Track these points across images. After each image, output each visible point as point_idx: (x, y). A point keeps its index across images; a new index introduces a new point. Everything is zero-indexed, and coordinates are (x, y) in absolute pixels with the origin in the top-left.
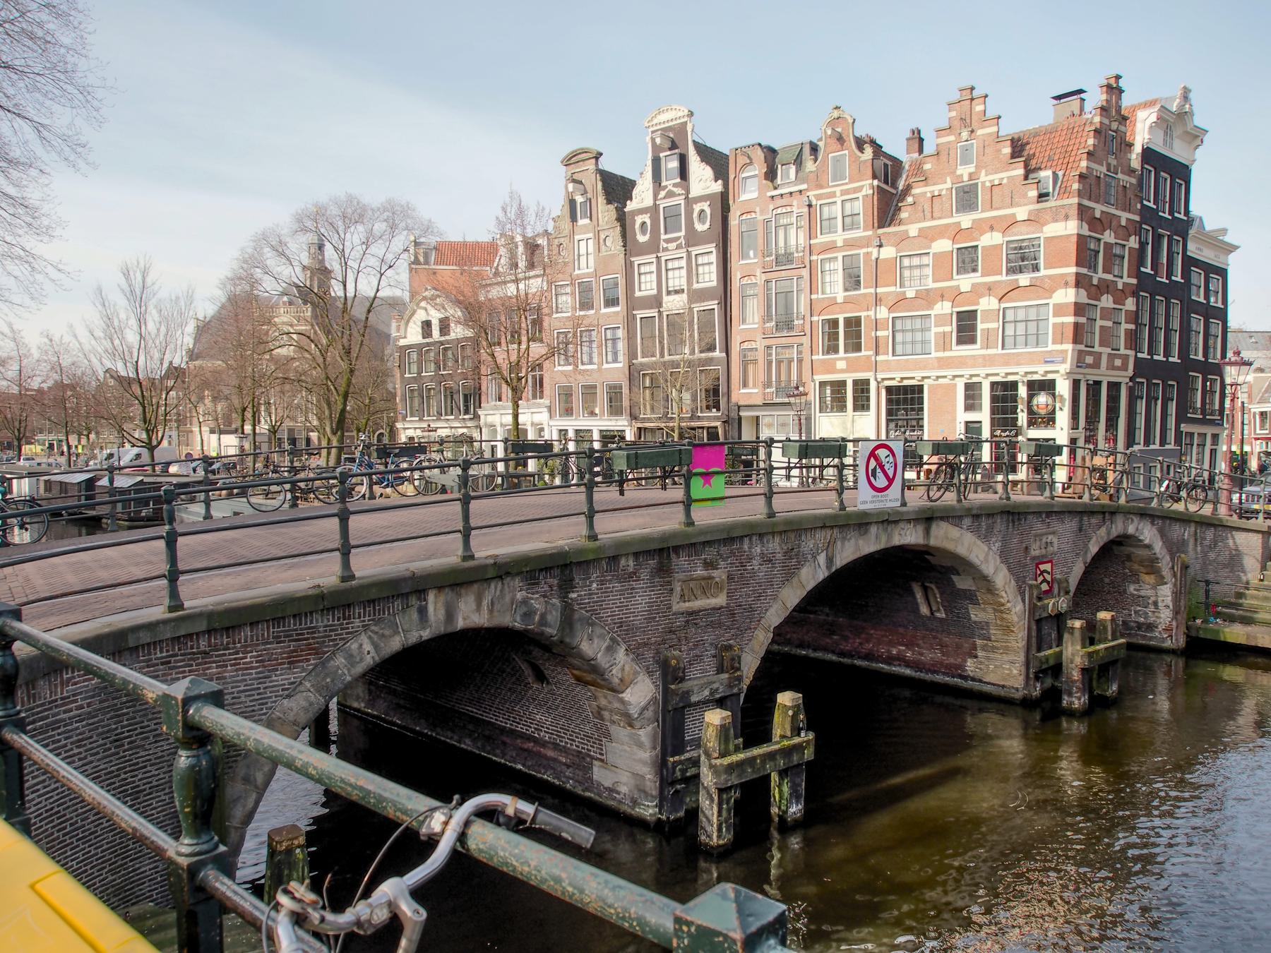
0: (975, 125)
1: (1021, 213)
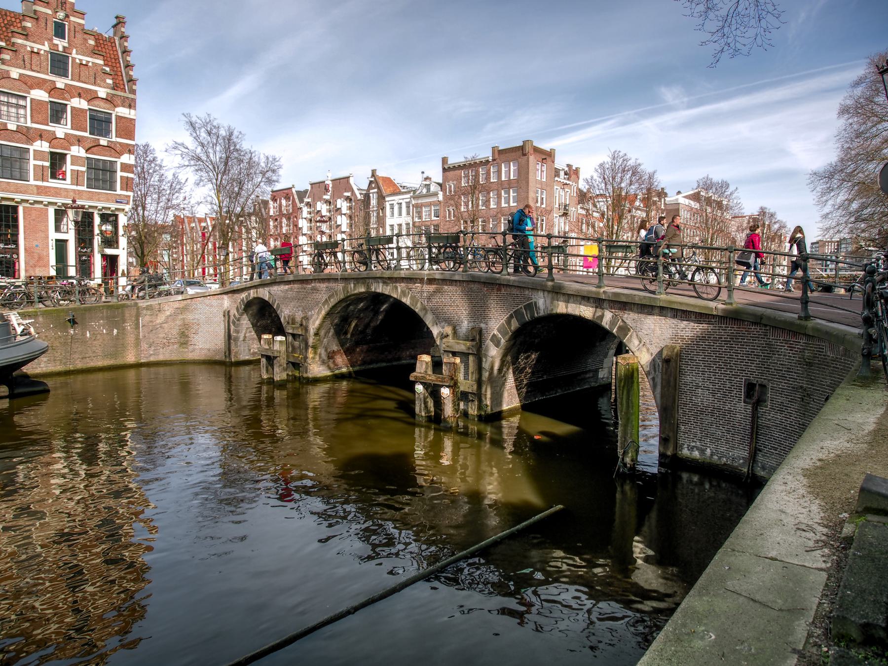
1: (102, 93)
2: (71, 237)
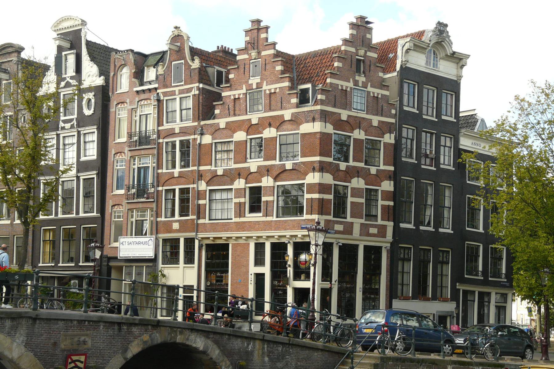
0: (261, 47)
1: (287, 114)
2: (266, 270)
